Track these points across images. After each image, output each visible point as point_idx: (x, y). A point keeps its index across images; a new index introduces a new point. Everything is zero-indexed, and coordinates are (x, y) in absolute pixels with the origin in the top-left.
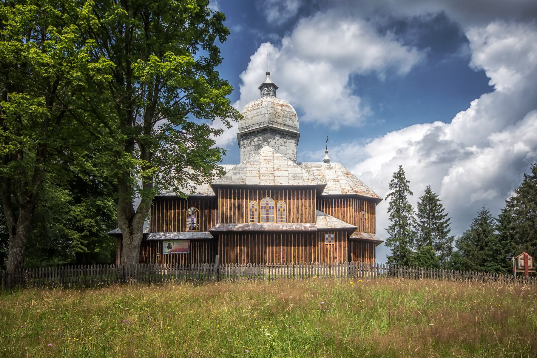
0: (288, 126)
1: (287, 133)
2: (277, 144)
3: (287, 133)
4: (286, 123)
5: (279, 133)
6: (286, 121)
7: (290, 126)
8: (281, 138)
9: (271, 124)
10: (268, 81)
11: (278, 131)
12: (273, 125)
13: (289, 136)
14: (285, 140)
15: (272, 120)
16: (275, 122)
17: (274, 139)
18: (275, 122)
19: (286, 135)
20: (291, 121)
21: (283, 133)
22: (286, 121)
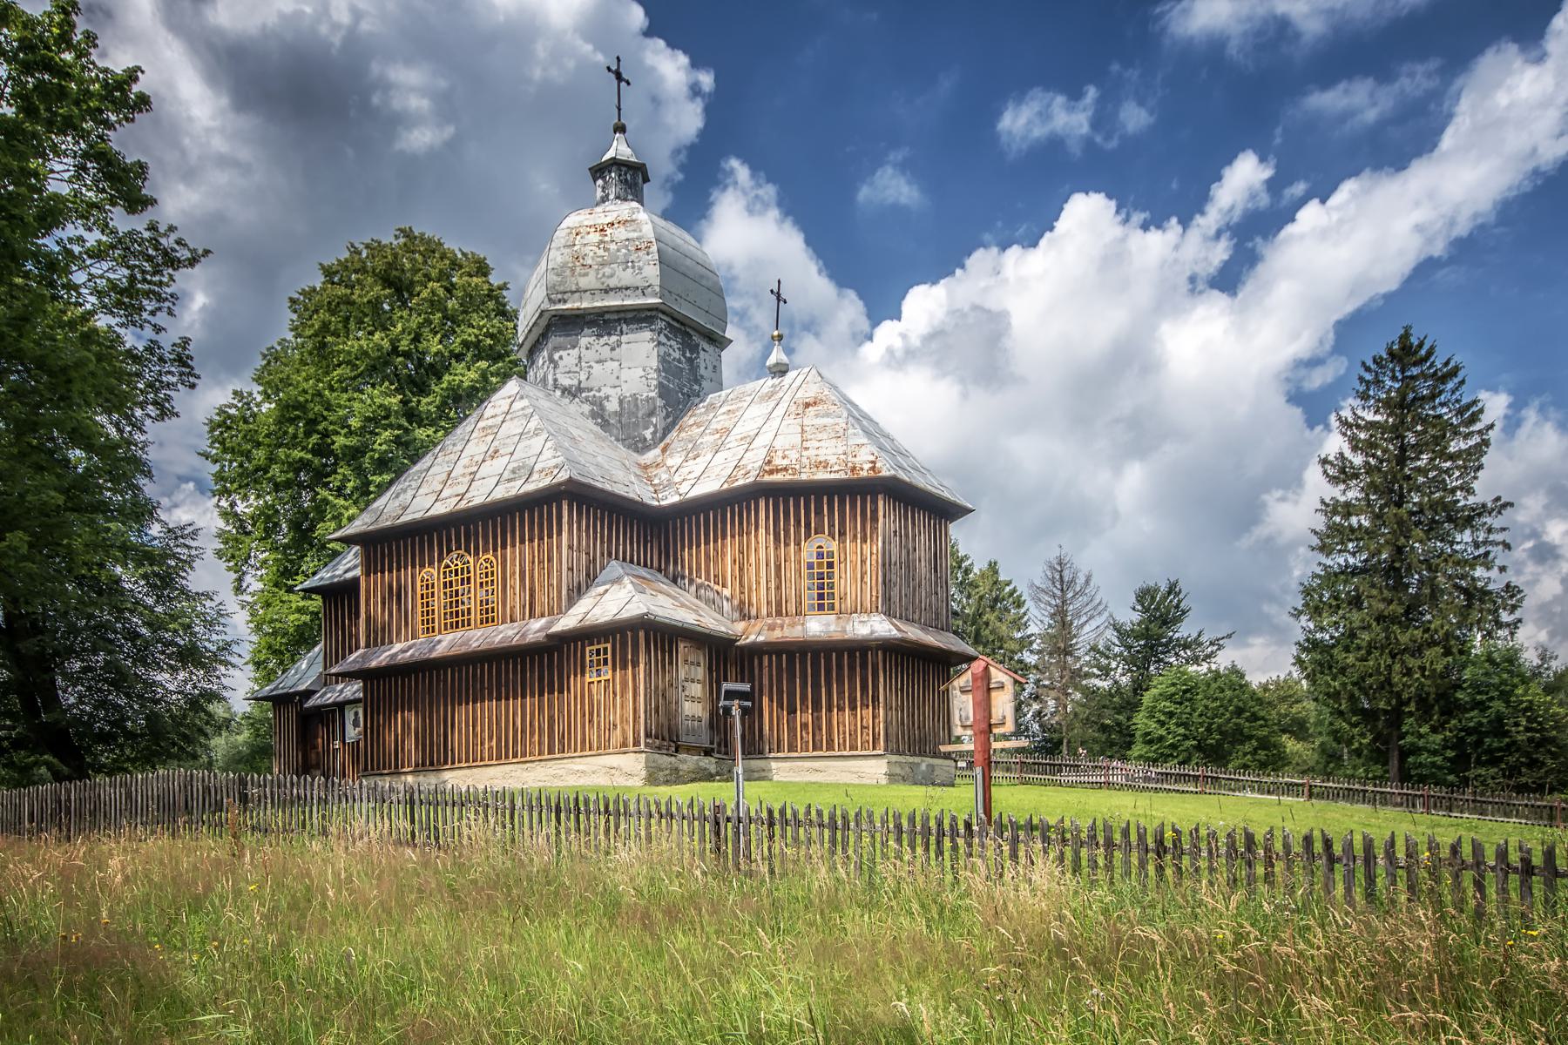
0: (620, 289)
1: (622, 315)
2: (584, 359)
3: (622, 315)
4: (613, 283)
5: (591, 324)
6: (612, 276)
7: (627, 288)
8: (599, 336)
9: (560, 301)
10: (619, 149)
11: (588, 318)
12: (565, 302)
13: (627, 322)
14: (614, 338)
15: (562, 289)
16: (573, 292)
17: (574, 347)
18: (573, 292)
19: (619, 320)
20: (630, 271)
21: (607, 317)
22: (612, 276)
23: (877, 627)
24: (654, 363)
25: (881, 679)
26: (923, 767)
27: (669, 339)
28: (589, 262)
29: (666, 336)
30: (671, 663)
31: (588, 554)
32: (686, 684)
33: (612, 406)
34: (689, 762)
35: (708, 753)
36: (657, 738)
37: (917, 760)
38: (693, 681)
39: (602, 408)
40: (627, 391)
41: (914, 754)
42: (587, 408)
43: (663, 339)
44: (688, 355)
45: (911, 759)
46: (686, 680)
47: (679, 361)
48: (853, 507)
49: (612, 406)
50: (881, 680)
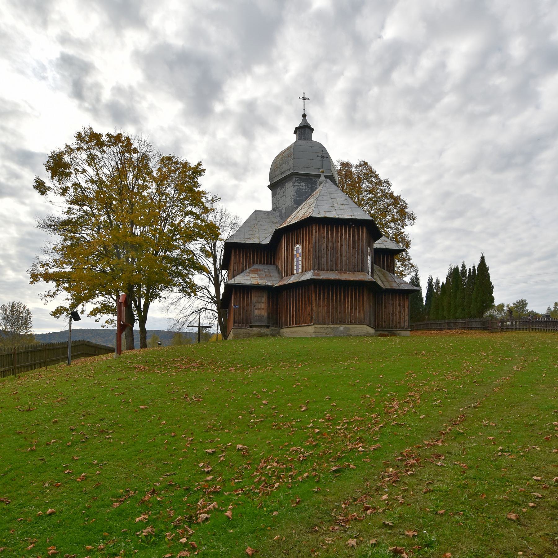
4: (283, 170)
23: (309, 276)
24: (293, 193)
25: (313, 296)
26: (342, 328)
27: (299, 183)
28: (278, 166)
29: (298, 182)
30: (248, 297)
31: (243, 264)
32: (256, 304)
33: (284, 211)
34: (255, 330)
35: (268, 327)
36: (239, 323)
37: (336, 326)
38: (260, 303)
39: (281, 212)
40: (287, 204)
41: (336, 323)
42: (278, 213)
43: (296, 184)
44: (310, 186)
45: (332, 326)
46: (256, 303)
47: (306, 189)
48: (306, 231)
49: (284, 211)
50: (313, 296)
